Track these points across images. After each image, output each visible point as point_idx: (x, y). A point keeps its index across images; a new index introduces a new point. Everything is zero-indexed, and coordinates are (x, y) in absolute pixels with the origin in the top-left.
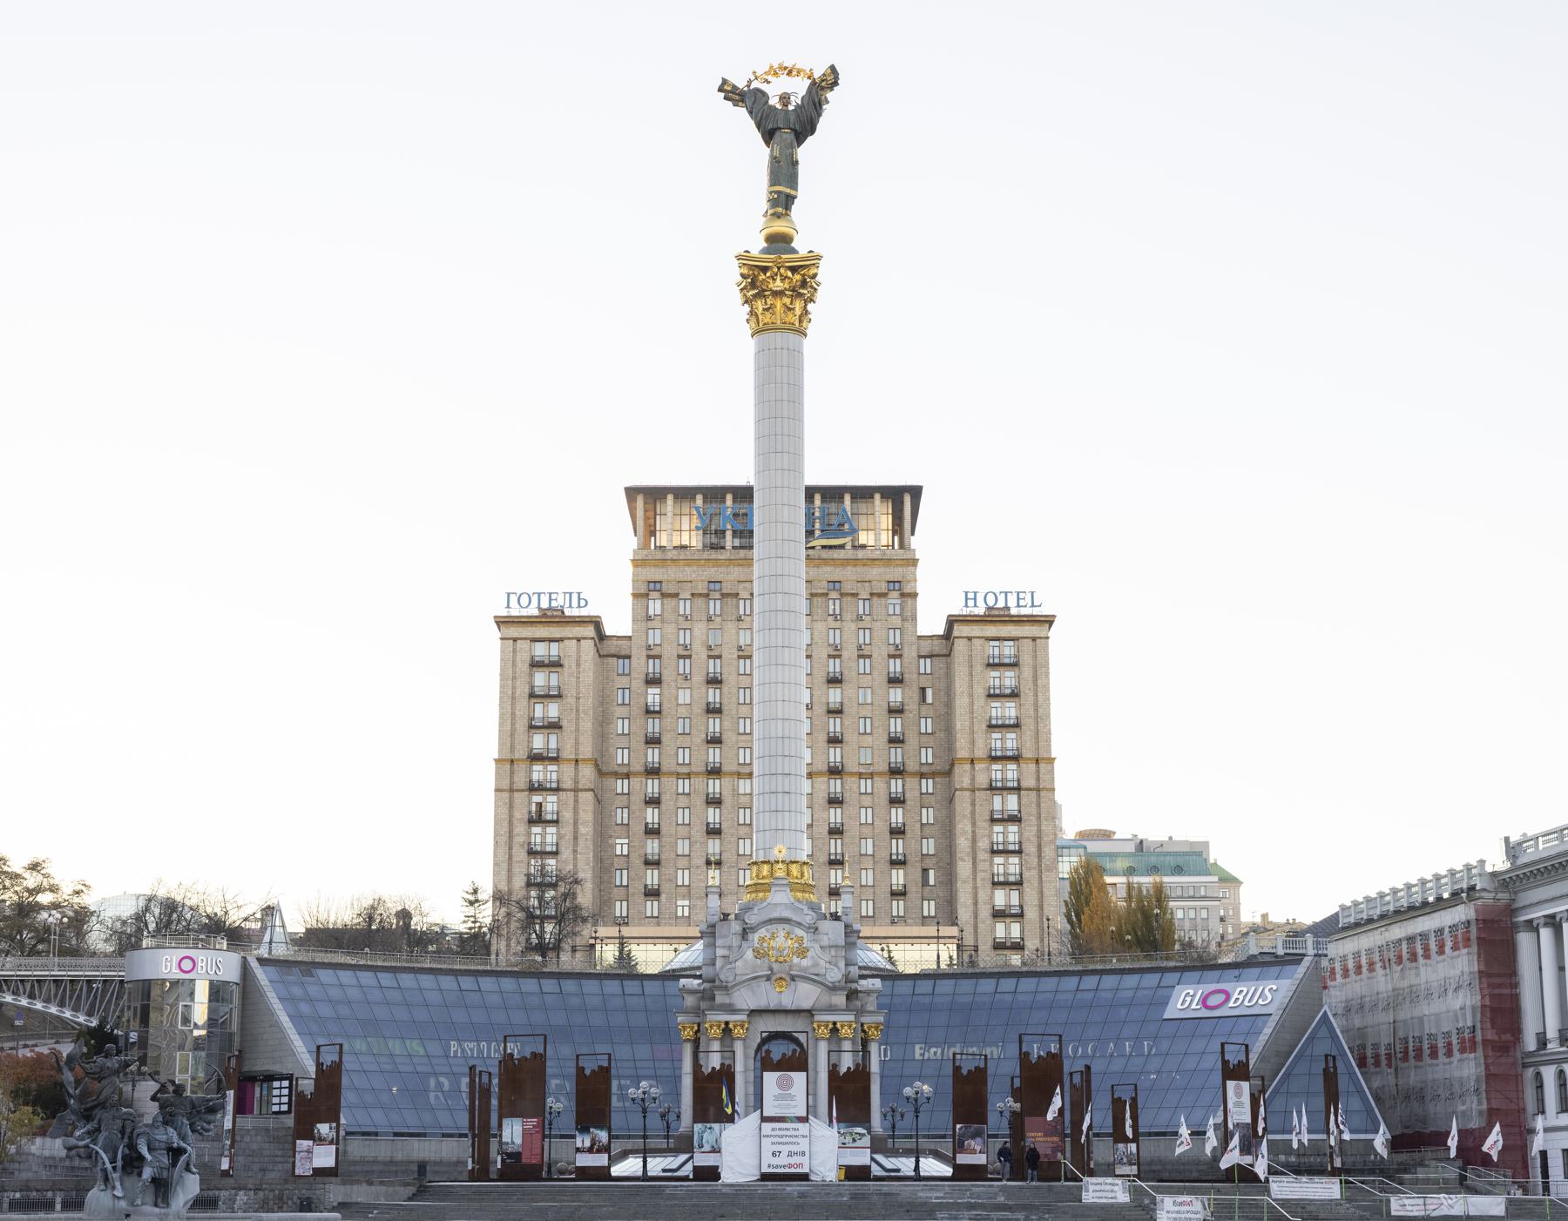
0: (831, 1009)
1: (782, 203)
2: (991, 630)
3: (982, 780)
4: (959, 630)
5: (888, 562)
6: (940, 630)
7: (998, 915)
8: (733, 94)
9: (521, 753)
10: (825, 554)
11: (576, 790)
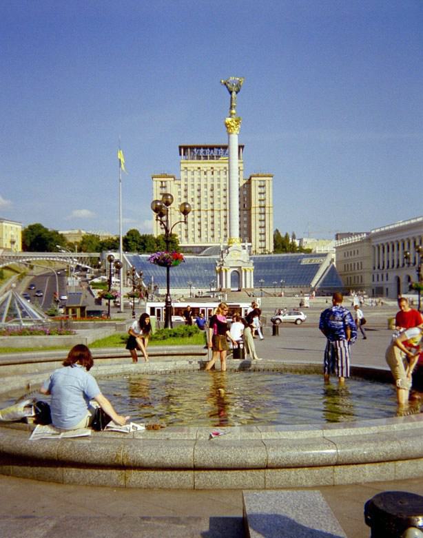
4: (252, 178)
6: (248, 178)
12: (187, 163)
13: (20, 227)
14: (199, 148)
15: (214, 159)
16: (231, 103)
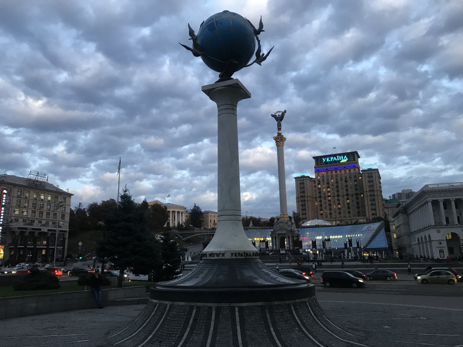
1: (279, 129)
2: (368, 172)
3: (368, 194)
7: (373, 214)
8: (272, 116)
9: (299, 196)
11: (308, 201)
12: (319, 167)
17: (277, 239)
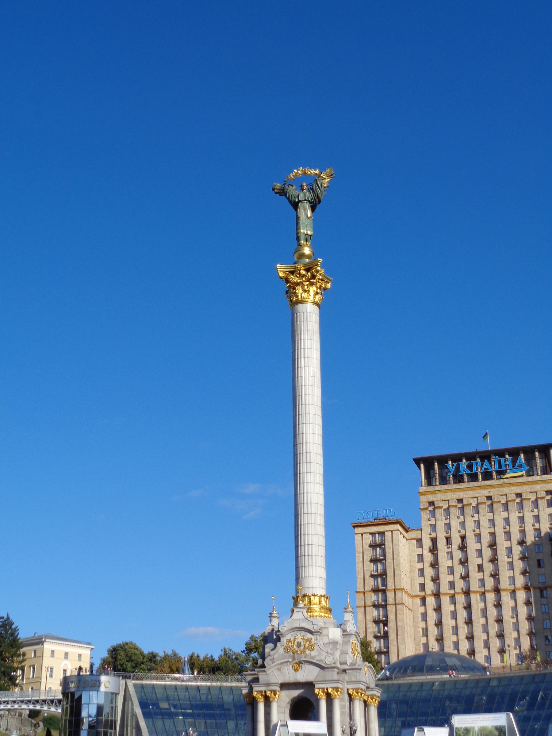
0: (324, 682)
5: (544, 481)
9: (368, 588)
10: (512, 481)
11: (395, 605)
12: (434, 492)
13: (88, 652)
14: (457, 458)
15: (491, 478)
16: (298, 228)
17: (275, 707)
